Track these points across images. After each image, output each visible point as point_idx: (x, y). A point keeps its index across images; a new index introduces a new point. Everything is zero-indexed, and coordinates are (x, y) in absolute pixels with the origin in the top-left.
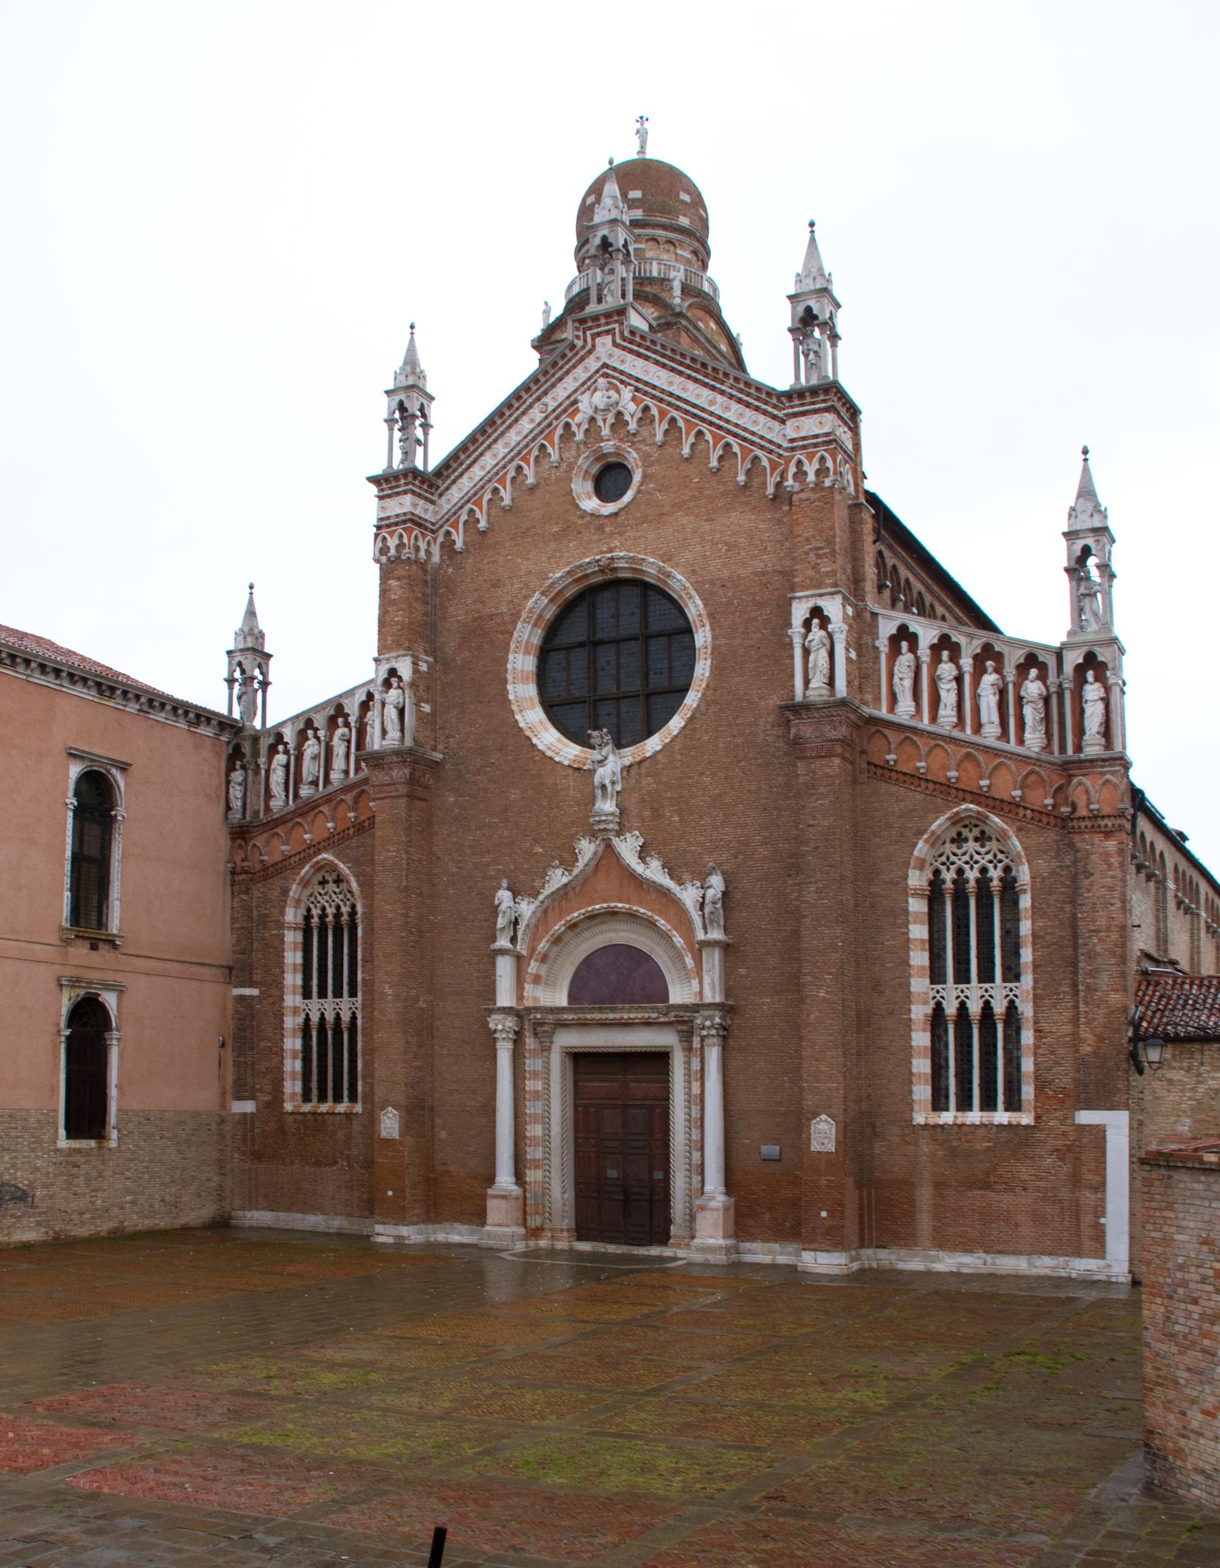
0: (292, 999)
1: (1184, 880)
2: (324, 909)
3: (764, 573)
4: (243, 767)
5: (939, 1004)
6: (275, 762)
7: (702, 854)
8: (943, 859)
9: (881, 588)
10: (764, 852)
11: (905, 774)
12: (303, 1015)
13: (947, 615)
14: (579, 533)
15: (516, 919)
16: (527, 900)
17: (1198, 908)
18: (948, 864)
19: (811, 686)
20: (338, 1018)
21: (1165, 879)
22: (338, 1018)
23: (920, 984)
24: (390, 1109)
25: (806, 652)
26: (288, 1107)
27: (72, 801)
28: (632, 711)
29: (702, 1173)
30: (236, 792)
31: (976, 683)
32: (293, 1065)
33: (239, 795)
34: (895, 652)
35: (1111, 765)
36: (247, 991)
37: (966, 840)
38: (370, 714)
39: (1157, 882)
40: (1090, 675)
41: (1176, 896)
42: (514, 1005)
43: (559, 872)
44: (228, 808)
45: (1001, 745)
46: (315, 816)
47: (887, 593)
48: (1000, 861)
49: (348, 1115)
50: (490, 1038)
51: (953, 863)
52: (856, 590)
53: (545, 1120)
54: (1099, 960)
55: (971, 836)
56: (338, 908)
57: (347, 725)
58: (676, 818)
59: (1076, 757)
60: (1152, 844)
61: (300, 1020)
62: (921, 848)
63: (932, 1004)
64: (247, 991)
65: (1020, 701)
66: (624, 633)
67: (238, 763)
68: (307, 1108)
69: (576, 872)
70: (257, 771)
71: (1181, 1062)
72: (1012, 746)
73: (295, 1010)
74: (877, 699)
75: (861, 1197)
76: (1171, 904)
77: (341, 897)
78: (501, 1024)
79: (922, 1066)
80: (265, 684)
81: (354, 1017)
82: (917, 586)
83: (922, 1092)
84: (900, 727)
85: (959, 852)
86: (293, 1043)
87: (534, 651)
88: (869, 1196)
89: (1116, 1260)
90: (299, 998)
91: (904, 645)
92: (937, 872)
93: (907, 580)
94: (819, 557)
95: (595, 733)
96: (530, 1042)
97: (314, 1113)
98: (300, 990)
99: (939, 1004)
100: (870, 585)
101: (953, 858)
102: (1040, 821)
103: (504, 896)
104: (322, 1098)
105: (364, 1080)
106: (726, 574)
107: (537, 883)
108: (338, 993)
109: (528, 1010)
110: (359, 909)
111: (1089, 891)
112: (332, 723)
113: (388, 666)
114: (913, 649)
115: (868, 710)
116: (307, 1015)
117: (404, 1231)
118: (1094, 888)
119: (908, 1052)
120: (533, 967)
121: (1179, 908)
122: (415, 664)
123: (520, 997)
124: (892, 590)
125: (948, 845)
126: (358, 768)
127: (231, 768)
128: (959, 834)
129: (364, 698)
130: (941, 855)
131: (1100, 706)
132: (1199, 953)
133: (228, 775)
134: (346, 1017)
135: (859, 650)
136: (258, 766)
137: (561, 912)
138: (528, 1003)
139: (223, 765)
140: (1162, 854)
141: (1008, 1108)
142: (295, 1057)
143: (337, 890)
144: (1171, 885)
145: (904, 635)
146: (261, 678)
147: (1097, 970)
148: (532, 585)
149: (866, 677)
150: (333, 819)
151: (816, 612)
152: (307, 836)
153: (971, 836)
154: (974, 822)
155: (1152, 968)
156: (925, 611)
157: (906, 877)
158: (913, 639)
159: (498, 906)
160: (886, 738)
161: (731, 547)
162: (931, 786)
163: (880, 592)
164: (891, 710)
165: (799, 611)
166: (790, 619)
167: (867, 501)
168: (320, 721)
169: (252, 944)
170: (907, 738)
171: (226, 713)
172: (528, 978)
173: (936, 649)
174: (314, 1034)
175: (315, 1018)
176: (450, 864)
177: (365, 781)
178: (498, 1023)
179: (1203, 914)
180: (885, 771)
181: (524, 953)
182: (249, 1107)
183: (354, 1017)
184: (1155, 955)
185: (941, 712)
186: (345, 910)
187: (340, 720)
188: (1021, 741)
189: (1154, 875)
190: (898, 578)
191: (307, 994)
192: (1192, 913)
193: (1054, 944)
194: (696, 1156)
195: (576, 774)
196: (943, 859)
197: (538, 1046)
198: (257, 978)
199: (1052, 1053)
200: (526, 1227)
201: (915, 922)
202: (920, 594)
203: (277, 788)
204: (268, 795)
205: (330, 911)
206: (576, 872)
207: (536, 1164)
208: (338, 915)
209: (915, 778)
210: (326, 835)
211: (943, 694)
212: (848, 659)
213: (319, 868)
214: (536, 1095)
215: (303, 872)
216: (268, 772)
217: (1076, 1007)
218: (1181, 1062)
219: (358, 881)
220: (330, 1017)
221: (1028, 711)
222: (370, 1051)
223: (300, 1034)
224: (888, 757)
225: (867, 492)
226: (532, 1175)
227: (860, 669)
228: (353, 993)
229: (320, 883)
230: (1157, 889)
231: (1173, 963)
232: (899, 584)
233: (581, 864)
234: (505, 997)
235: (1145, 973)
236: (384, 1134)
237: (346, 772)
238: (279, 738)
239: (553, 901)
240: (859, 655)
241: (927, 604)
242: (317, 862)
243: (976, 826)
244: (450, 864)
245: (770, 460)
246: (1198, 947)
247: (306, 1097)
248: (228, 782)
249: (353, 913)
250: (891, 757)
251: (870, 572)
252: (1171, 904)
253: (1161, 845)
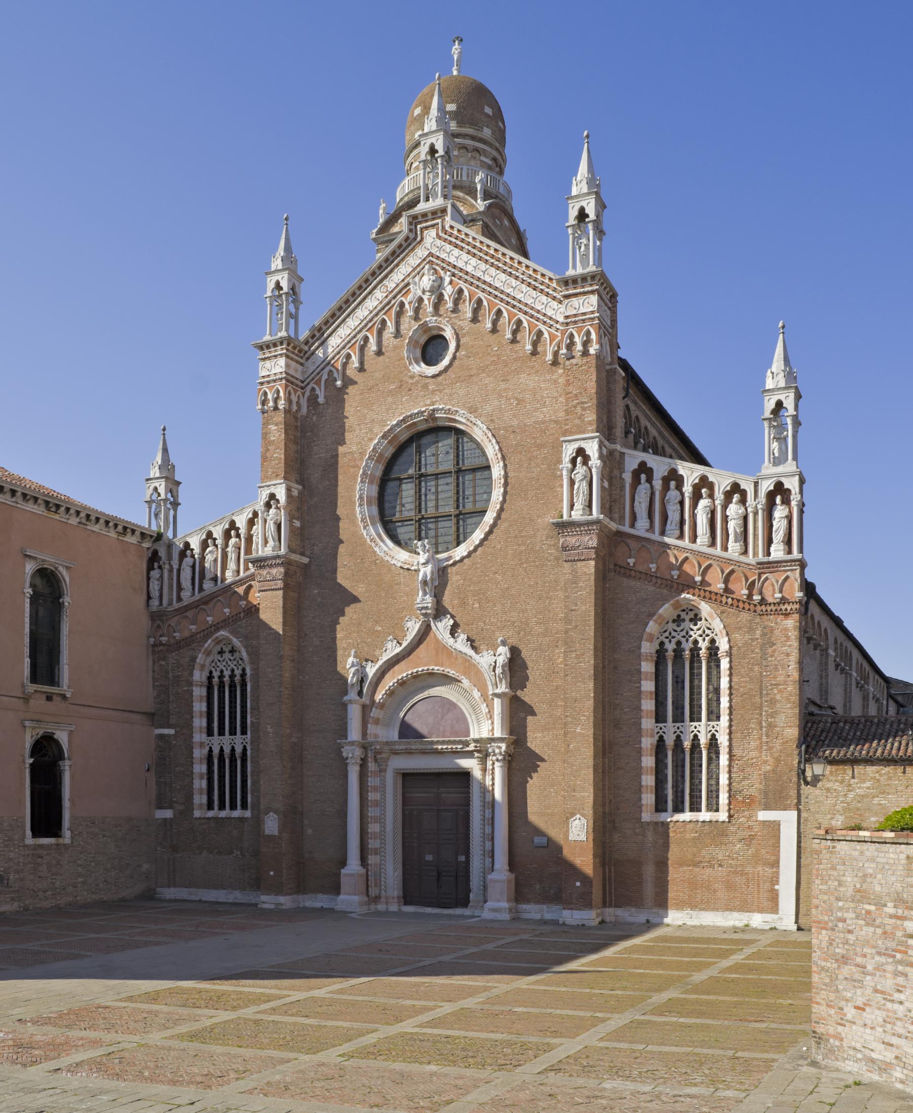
0: (199, 737)
1: (841, 649)
2: (222, 671)
3: (543, 422)
4: (160, 567)
5: (661, 738)
6: (184, 563)
8: (667, 634)
9: (627, 433)
11: (641, 572)
12: (207, 749)
13: (673, 455)
14: (410, 390)
17: (850, 669)
18: (670, 638)
19: (575, 508)
20: (233, 750)
21: (827, 649)
22: (233, 750)
23: (648, 723)
24: (271, 814)
25: (572, 482)
26: (197, 814)
27: (29, 591)
28: (448, 527)
29: (493, 857)
30: (155, 586)
31: (694, 505)
32: (200, 784)
33: (157, 588)
34: (636, 481)
35: (791, 566)
36: (166, 731)
37: (684, 620)
38: (255, 527)
39: (821, 650)
40: (778, 499)
41: (835, 661)
42: (360, 740)
44: (149, 598)
45: (710, 551)
46: (216, 604)
47: (631, 437)
48: (708, 635)
49: (241, 819)
50: (343, 763)
51: (674, 637)
52: (609, 435)
53: (381, 820)
54: (778, 705)
55: (687, 618)
56: (233, 671)
57: (238, 536)
58: (477, 605)
59: (766, 559)
60: (819, 622)
61: (206, 751)
62: (652, 627)
63: (657, 737)
64: (166, 731)
65: (725, 519)
66: (442, 469)
67: (156, 565)
68: (211, 814)
69: (405, 644)
70: (171, 570)
71: (836, 776)
72: (718, 551)
73: (202, 745)
74: (622, 518)
75: (604, 873)
76: (831, 666)
77: (235, 663)
78: (352, 754)
79: (649, 780)
80: (175, 504)
81: (245, 749)
82: (653, 432)
83: (648, 799)
84: (638, 538)
85: (678, 629)
86: (200, 768)
87: (377, 481)
88: (610, 871)
89: (786, 919)
90: (204, 735)
91: (643, 477)
92: (662, 644)
93: (646, 428)
94: (584, 409)
95: (420, 543)
96: (372, 766)
97: (216, 819)
98: (205, 730)
99: (661, 738)
100: (619, 431)
101: (674, 634)
102: (738, 606)
104: (222, 807)
105: (252, 794)
106: (515, 423)
107: (377, 653)
108: (233, 732)
109: (371, 744)
110: (248, 671)
111: (772, 656)
112: (227, 535)
113: (268, 492)
114: (649, 480)
115: (613, 526)
116: (211, 748)
117: (282, 899)
118: (777, 653)
119: (638, 771)
120: (375, 713)
121: (837, 669)
122: (289, 490)
123: (364, 734)
124: (635, 436)
125: (670, 624)
126: (247, 569)
127: (150, 568)
128: (679, 616)
129: (250, 516)
130: (665, 631)
131: (785, 523)
132: (850, 701)
133: (148, 573)
134: (239, 750)
135: (610, 480)
136: (171, 566)
138: (370, 739)
139: (144, 566)
140: (826, 630)
141: (709, 809)
142: (202, 778)
143: (232, 658)
144: (832, 652)
145: (643, 469)
146: (172, 499)
147: (776, 713)
148: (375, 430)
149: (615, 501)
150: (230, 607)
151: (581, 452)
152: (209, 619)
153: (687, 618)
154: (690, 607)
155: (816, 710)
156: (658, 451)
157: (640, 648)
158: (649, 472)
160: (627, 545)
161: (520, 401)
162: (659, 581)
163: (626, 437)
164: (632, 526)
165: (569, 451)
166: (561, 457)
167: (620, 366)
168: (218, 533)
169: (169, 696)
170: (643, 546)
171: (147, 526)
172: (371, 720)
173: (666, 480)
174: (216, 761)
175: (216, 751)
176: (315, 639)
177: (252, 577)
178: (346, 752)
179: (854, 674)
180: (625, 571)
182: (168, 814)
183: (245, 749)
184: (819, 702)
185: (668, 527)
186: (238, 672)
187: (233, 532)
188: (725, 549)
189: (820, 645)
190: (639, 426)
191: (210, 733)
192: (846, 673)
193: (745, 694)
194: (488, 845)
195: (406, 573)
196: (667, 634)
197: (377, 769)
198: (172, 721)
199: (743, 771)
200: (368, 895)
201: (646, 679)
202: (654, 438)
203: (186, 583)
204: (180, 588)
205: (227, 673)
207: (376, 852)
208: (232, 676)
209: (648, 576)
210: (223, 618)
211: (670, 514)
212: (602, 488)
213: (218, 641)
214: (376, 804)
215: (206, 645)
216: (179, 570)
217: (760, 739)
218: (836, 776)
219: (247, 652)
220: (227, 751)
221: (732, 525)
222: (257, 773)
223: (205, 762)
224: (629, 560)
225: (620, 358)
226: (372, 859)
227: (610, 495)
228: (244, 732)
229: (219, 653)
230: (822, 655)
231: (832, 708)
232: (640, 430)
234: (354, 734)
235: (812, 714)
236: (267, 832)
237: (238, 572)
238: (187, 545)
240: (610, 484)
241: (660, 446)
242: (217, 638)
243: (691, 610)
244: (315, 639)
245: (549, 333)
246: (850, 697)
247: (210, 807)
248: (148, 579)
249: (243, 675)
250: (631, 561)
251: (620, 422)
252: (831, 666)
253: (826, 623)
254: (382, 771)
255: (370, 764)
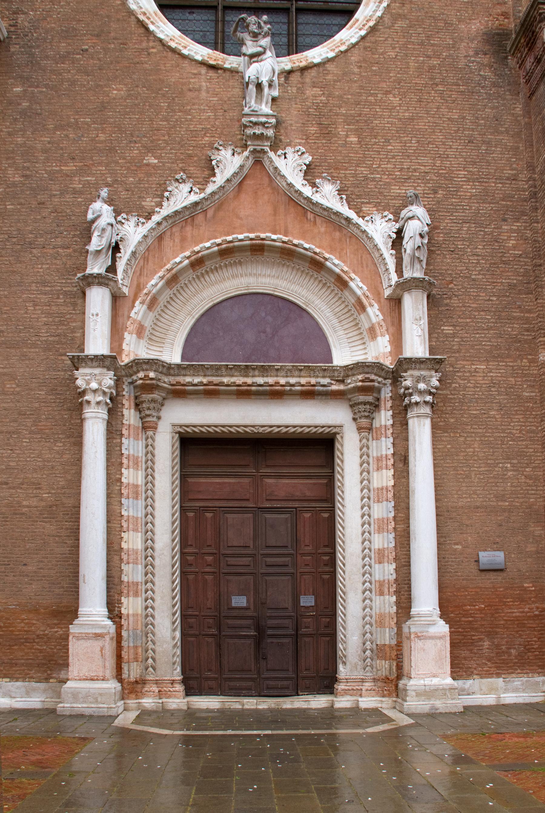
7: (386, 184)
10: (469, 189)
15: (117, 244)
16: (133, 220)
43: (185, 188)
103: (101, 211)
137: (183, 239)
159: (93, 221)
181: (125, 290)
206: (211, 188)
233: (220, 179)
239: (173, 225)
254: (148, 427)
255: (126, 412)
